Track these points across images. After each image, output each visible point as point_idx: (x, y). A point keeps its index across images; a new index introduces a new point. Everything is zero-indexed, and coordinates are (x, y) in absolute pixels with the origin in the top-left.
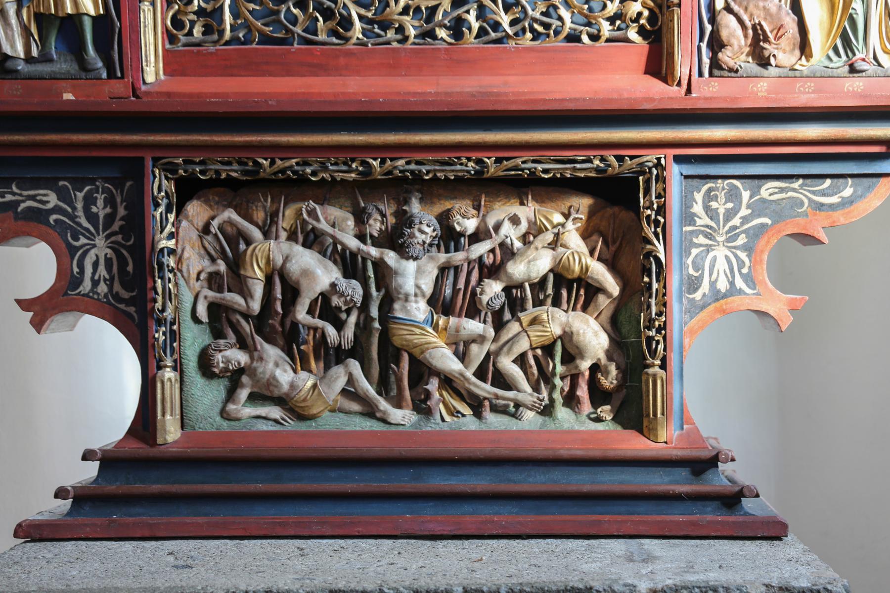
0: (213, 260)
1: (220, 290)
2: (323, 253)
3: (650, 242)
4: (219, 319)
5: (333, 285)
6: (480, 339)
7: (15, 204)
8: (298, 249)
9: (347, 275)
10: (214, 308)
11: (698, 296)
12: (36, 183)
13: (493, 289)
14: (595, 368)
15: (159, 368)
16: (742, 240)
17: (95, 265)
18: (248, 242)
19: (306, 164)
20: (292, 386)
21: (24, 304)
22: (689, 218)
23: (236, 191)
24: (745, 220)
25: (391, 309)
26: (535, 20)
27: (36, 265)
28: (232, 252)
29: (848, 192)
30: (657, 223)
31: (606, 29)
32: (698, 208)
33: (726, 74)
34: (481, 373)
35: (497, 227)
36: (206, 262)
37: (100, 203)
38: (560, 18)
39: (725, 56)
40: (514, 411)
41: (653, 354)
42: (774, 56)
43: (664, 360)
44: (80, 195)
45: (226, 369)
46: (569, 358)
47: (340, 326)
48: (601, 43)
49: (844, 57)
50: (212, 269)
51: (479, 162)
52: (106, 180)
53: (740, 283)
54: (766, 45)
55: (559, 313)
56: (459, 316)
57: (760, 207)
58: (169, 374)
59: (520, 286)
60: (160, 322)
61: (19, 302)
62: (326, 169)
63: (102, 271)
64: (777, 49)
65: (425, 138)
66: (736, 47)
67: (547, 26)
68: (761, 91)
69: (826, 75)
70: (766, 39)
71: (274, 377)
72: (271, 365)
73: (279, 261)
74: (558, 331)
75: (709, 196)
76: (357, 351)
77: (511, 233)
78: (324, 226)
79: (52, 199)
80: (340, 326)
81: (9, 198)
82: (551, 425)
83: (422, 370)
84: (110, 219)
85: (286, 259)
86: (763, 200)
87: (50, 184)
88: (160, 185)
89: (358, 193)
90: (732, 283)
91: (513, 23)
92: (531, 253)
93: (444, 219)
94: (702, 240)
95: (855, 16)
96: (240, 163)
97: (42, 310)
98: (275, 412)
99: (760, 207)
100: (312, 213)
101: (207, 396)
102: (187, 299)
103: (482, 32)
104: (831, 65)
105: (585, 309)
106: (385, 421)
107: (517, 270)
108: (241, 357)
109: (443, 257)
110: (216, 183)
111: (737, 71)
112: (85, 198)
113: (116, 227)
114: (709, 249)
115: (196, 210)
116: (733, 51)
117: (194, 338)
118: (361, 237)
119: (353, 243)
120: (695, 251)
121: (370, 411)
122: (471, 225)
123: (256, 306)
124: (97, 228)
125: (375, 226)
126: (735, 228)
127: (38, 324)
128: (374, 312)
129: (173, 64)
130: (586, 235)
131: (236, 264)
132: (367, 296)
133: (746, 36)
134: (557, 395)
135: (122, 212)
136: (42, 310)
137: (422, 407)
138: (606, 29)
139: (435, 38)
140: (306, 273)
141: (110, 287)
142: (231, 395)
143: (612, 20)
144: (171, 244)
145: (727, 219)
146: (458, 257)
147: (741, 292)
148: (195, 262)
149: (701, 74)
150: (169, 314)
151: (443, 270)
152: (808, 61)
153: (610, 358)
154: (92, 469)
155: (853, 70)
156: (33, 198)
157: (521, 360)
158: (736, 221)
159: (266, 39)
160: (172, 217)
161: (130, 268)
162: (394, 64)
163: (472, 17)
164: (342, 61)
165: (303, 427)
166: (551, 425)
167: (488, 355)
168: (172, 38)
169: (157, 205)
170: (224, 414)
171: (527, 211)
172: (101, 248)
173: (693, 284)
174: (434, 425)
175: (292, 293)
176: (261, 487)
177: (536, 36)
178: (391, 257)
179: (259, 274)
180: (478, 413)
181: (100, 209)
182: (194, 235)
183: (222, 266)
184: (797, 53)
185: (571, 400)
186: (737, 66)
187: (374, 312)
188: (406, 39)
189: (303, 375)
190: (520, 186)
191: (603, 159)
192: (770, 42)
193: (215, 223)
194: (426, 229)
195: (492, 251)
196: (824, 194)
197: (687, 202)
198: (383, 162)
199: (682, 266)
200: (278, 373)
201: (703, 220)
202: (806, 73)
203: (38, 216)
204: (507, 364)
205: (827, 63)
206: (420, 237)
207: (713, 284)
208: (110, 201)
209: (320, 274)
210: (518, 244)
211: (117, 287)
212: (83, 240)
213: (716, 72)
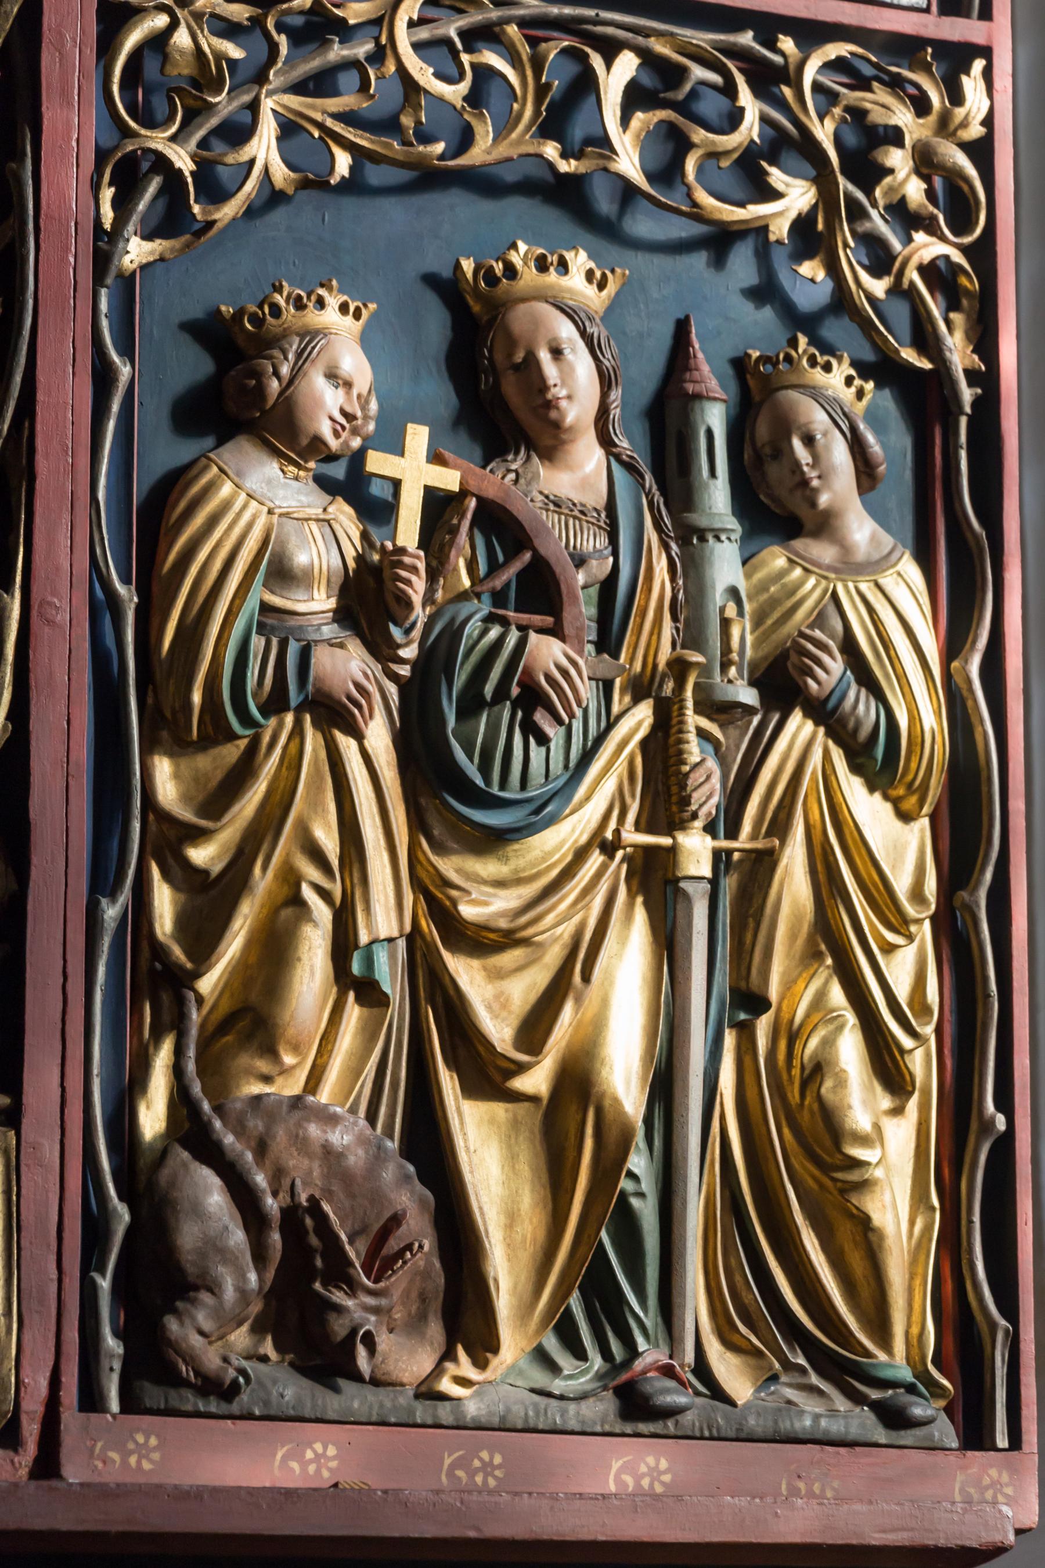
33: (191, 1401)
42: (368, 1335)
49: (597, 1362)
54: (338, 1297)
64: (376, 1310)
66: (229, 1293)
70: (339, 1273)
95: (635, 1202)
104: (558, 1386)
111: (231, 1392)
116: (218, 1313)
133: (259, 1256)
149: (91, 1400)
152: (481, 1364)
184: (435, 1330)
186: (232, 1373)
192: (352, 1287)
202: (472, 1409)
205: (540, 1378)
213: (152, 1394)
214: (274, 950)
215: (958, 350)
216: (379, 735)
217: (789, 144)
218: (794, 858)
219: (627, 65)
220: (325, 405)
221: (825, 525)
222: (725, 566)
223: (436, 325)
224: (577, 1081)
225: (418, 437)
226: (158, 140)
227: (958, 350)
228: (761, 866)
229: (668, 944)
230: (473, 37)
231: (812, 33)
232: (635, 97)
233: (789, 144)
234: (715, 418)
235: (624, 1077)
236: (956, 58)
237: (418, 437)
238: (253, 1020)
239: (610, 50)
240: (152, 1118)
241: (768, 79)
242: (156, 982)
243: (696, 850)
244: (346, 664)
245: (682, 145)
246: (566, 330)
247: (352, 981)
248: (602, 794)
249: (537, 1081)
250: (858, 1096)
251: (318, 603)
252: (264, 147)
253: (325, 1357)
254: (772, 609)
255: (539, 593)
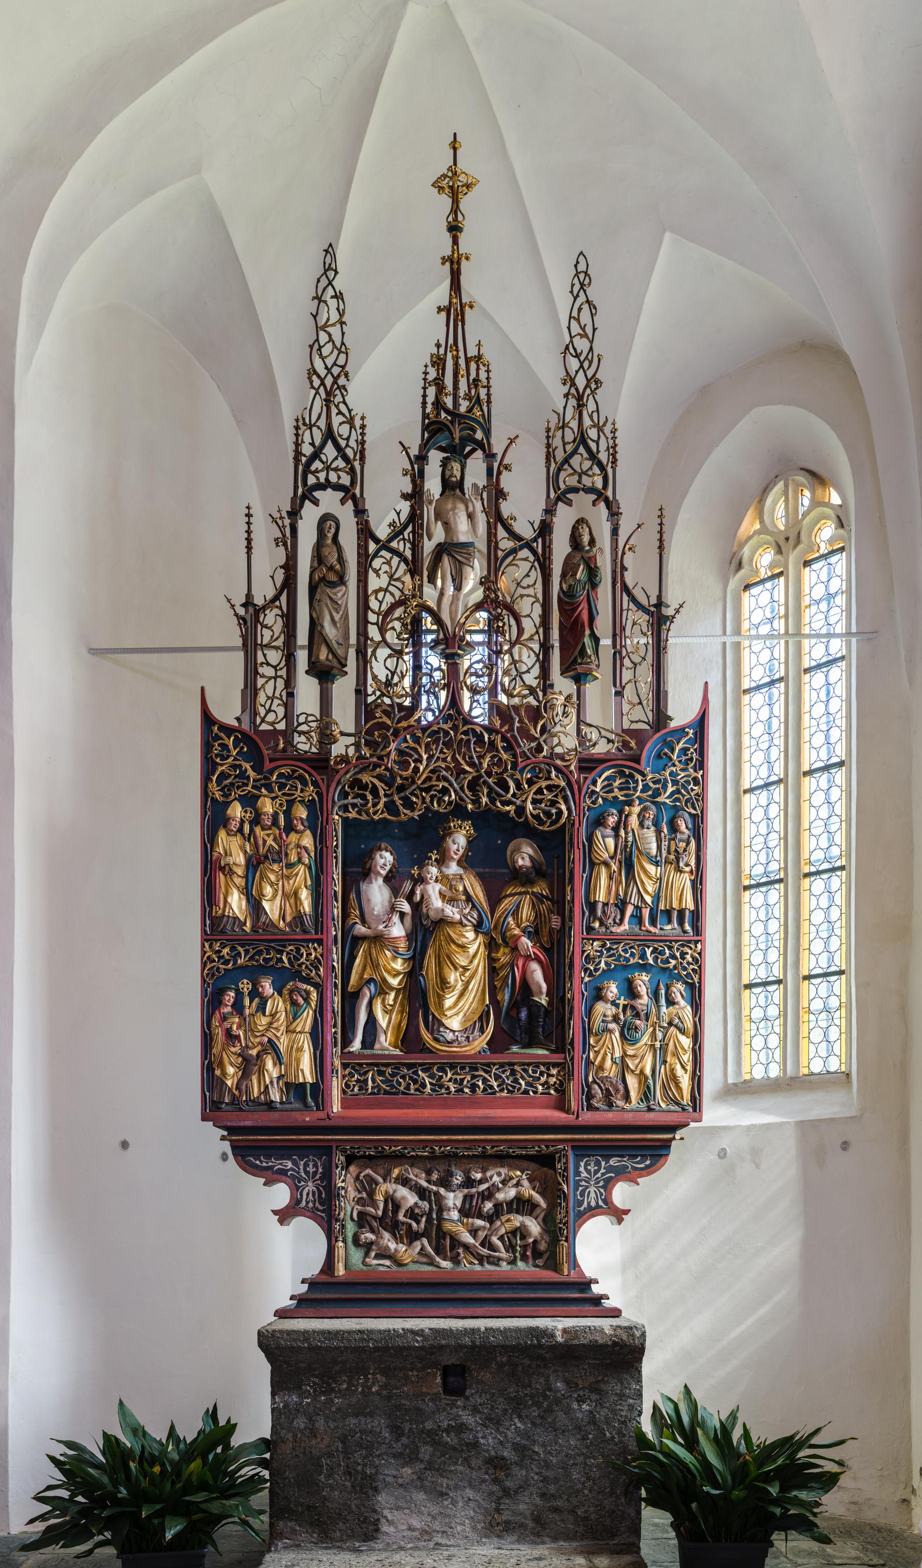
0: (360, 1192)
1: (364, 1205)
2: (410, 1189)
3: (561, 1184)
4: (363, 1220)
5: (416, 1203)
6: (484, 1228)
7: (273, 1167)
8: (400, 1187)
9: (420, 1199)
10: (360, 1214)
11: (582, 1209)
12: (282, 1157)
13: (488, 1206)
14: (535, 1242)
15: (336, 1241)
16: (601, 1183)
17: (308, 1194)
18: (377, 1184)
19: (405, 1148)
20: (396, 1250)
21: (275, 1212)
22: (578, 1173)
23: (369, 1160)
24: (603, 1174)
25: (442, 1214)
26: (508, 1084)
27: (281, 1194)
28: (368, 1188)
29: (648, 1162)
30: (564, 1175)
31: (540, 1088)
32: (582, 1169)
34: (483, 1244)
35: (491, 1177)
36: (357, 1193)
37: (311, 1166)
38: (520, 1084)
39: (594, 1102)
40: (496, 1261)
41: (562, 1235)
43: (567, 1238)
44: (302, 1163)
45: (366, 1242)
46: (523, 1237)
47: (418, 1222)
48: (538, 1095)
50: (360, 1196)
51: (484, 1148)
52: (314, 1156)
53: (601, 1203)
55: (520, 1218)
56: (473, 1218)
57: (609, 1169)
58: (341, 1244)
59: (501, 1204)
60: (337, 1220)
61: (273, 1211)
62: (414, 1151)
63: (311, 1197)
65: (460, 1137)
67: (514, 1087)
68: (609, 1117)
69: (637, 1111)
71: (388, 1246)
72: (386, 1241)
73: (391, 1192)
74: (518, 1225)
75: (586, 1165)
76: (426, 1234)
77: (496, 1179)
78: (412, 1176)
79: (290, 1165)
80: (418, 1222)
81: (270, 1164)
82: (515, 1269)
83: (456, 1242)
84: (315, 1173)
85: (395, 1191)
86: (611, 1166)
87: (289, 1158)
88: (340, 1159)
89: (428, 1163)
90: (597, 1203)
91: (498, 1086)
92: (507, 1189)
93: (467, 1174)
94: (584, 1183)
96: (375, 1148)
97: (284, 1216)
98: (387, 1262)
99: (609, 1169)
100: (406, 1170)
101: (356, 1256)
102: (349, 1209)
103: (485, 1090)
105: (530, 1215)
106: (439, 1267)
107: (500, 1196)
108: (371, 1236)
109: (466, 1191)
110: (364, 1156)
112: (304, 1164)
113: (317, 1177)
114: (587, 1187)
115: (353, 1169)
117: (351, 1228)
118: (429, 1182)
119: (425, 1184)
120: (581, 1188)
121: (432, 1263)
122: (479, 1176)
123: (380, 1213)
124: (308, 1177)
125: (435, 1176)
126: (598, 1178)
127: (281, 1222)
128: (434, 1216)
129: (345, 1104)
130: (530, 1180)
131: (371, 1194)
132: (431, 1209)
134: (518, 1254)
135: (320, 1170)
136: (284, 1216)
137: (456, 1260)
138: (540, 1088)
139: (463, 1092)
140: (404, 1198)
141: (314, 1204)
142: (367, 1254)
143: (543, 1085)
144: (343, 1184)
145: (595, 1174)
146: (474, 1190)
147: (601, 1207)
148: (352, 1193)
149: (583, 1110)
150: (342, 1216)
151: (465, 1197)
153: (542, 1237)
154: (305, 1287)
155: (650, 1109)
156: (281, 1164)
157: (501, 1238)
158: (599, 1175)
159: (386, 1092)
160: (343, 1173)
161: (323, 1196)
162: (445, 1104)
163: (480, 1083)
164: (421, 1102)
165: (401, 1269)
166: (515, 1269)
167: (486, 1236)
168: (344, 1092)
169: (337, 1167)
170: (364, 1263)
171: (504, 1171)
172: (311, 1187)
173: (580, 1203)
174: (461, 1268)
175: (397, 1207)
176: (383, 1296)
177: (509, 1091)
178: (442, 1191)
179: (382, 1199)
180: (481, 1264)
181: (311, 1169)
182: (352, 1180)
183: (364, 1195)
185: (524, 1258)
187: (434, 1216)
188: (450, 1093)
189: (401, 1245)
190: (501, 1159)
191: (539, 1147)
193: (362, 1175)
194: (458, 1179)
195: (488, 1188)
196: (637, 1163)
197: (577, 1167)
198: (440, 1148)
199: (575, 1195)
200: (390, 1244)
201: (584, 1174)
203: (283, 1172)
204: (495, 1240)
206: (456, 1182)
207: (589, 1203)
208: (315, 1166)
209: (409, 1198)
210: (500, 1185)
211: (317, 1204)
212: (303, 1183)
214: (604, 1059)
215: (696, 980)
216: (617, 1034)
217: (673, 957)
218: (671, 1044)
219: (651, 949)
220: (610, 996)
221: (677, 1003)
222: (664, 1009)
223: (626, 984)
224: (642, 1072)
225: (622, 998)
226: (589, 966)
227: (696, 980)
228: (667, 1044)
229: (655, 1056)
230: (630, 948)
231: (676, 941)
232: (652, 953)
233: (673, 957)
234: (663, 992)
235: (648, 1071)
236: (696, 942)
237: (622, 998)
238: (601, 1068)
239: (648, 947)
240: (590, 1079)
241: (670, 948)
242: (589, 1063)
243: (658, 1044)
244: (612, 1026)
245: (657, 958)
246: (641, 983)
247: (614, 1062)
248: (646, 1039)
249: (638, 1072)
250: (679, 1071)
251: (610, 1018)
252: (603, 965)
253: (610, 1105)
254: (670, 1014)
255: (637, 1015)
